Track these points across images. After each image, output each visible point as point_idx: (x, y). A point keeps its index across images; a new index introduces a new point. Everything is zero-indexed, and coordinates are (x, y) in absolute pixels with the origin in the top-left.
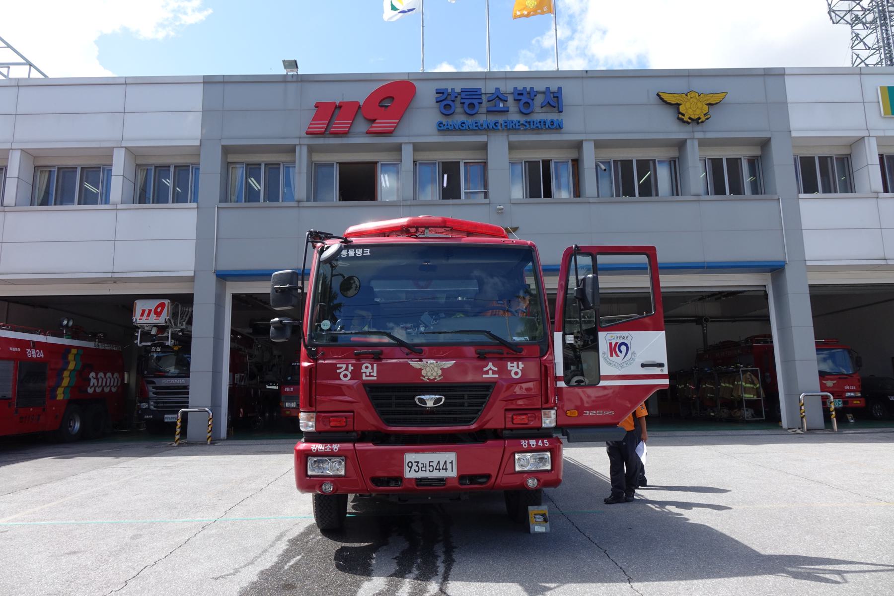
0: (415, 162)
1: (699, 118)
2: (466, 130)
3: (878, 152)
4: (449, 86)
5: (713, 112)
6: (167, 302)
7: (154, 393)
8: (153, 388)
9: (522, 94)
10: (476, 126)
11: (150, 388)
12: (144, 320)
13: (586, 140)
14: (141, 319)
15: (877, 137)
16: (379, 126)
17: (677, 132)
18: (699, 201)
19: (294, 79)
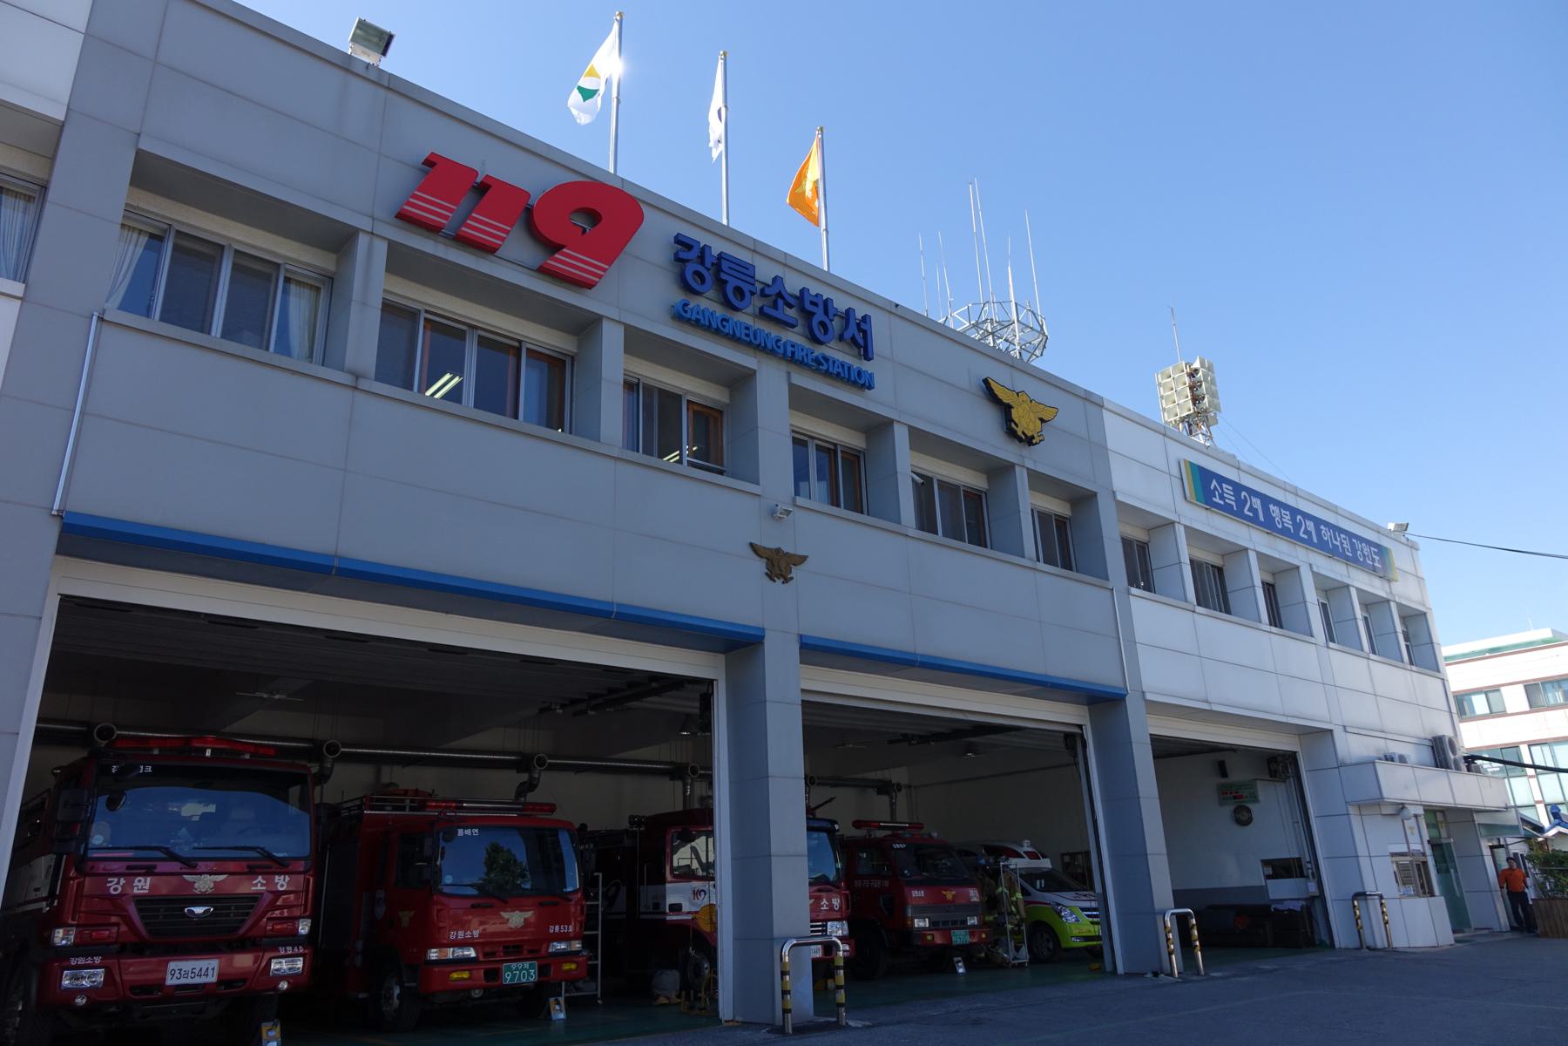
1: (1033, 437)
4: (703, 239)
9: (816, 304)
10: (747, 335)
13: (898, 422)
16: (561, 261)
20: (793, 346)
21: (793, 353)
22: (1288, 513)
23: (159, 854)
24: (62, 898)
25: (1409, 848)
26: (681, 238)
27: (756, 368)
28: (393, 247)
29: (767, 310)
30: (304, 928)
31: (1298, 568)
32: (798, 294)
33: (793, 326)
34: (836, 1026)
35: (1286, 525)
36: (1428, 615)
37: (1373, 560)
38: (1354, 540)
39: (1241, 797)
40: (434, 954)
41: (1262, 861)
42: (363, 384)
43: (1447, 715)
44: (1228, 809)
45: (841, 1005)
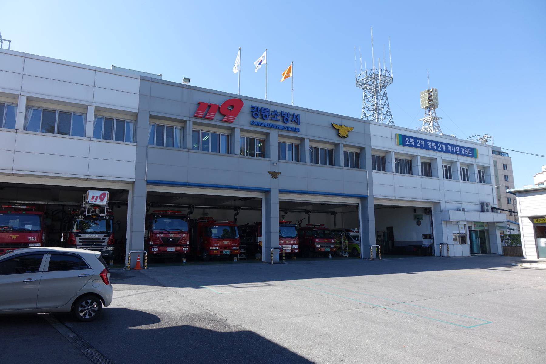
1: (345, 136)
2: (263, 126)
3: (395, 157)
5: (349, 134)
6: (107, 192)
7: (80, 242)
8: (80, 239)
9: (285, 115)
10: (268, 126)
11: (77, 239)
12: (93, 202)
14: (92, 201)
15: (395, 152)
17: (337, 140)
18: (343, 169)
19: (187, 87)
21: (279, 128)
23: (164, 230)
24: (150, 237)
25: (459, 232)
27: (270, 132)
29: (273, 119)
30: (188, 243)
34: (283, 263)
35: (433, 147)
37: (469, 153)
38: (461, 148)
39: (419, 218)
40: (211, 248)
43: (492, 196)
44: (416, 221)
45: (284, 260)
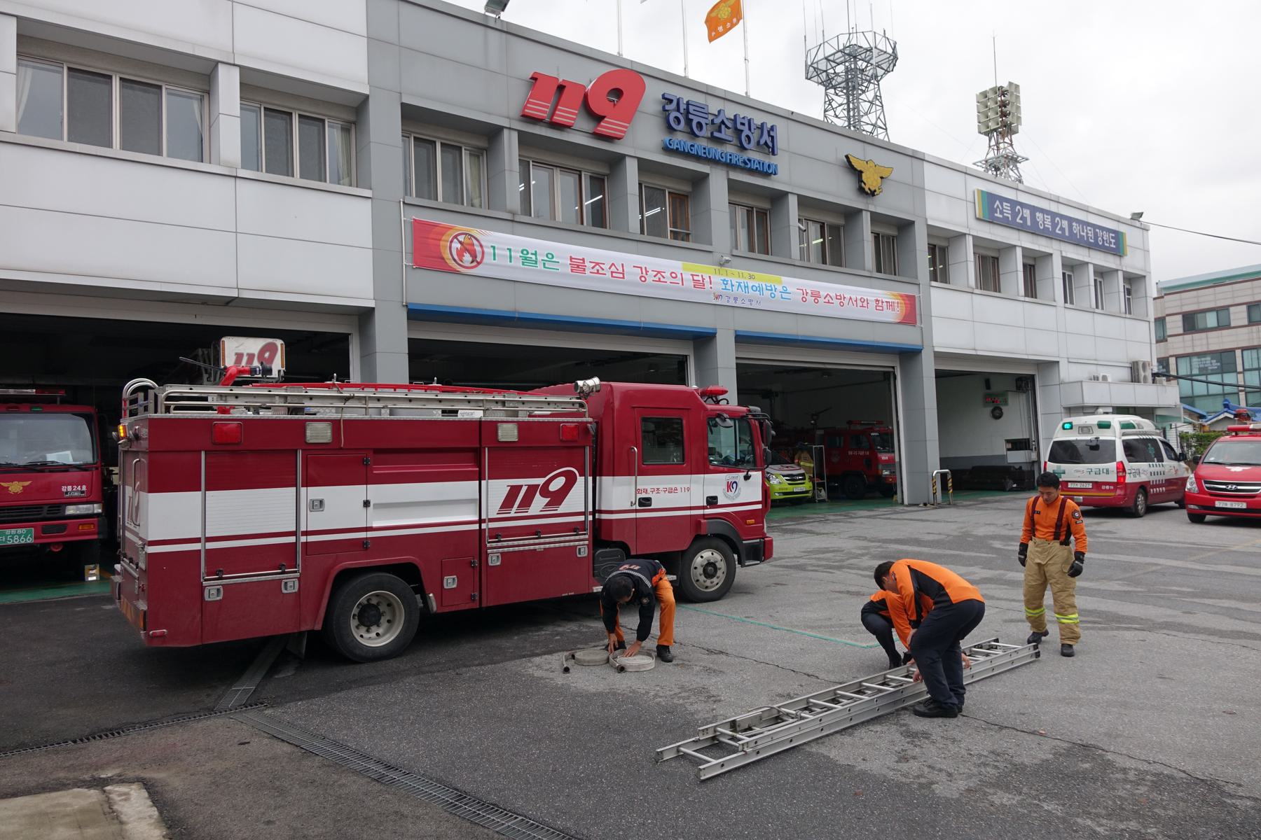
0: (640, 185)
1: (875, 191)
6: (279, 343)
9: (743, 124)
10: (705, 153)
16: (604, 128)
20: (730, 155)
21: (731, 160)
22: (1049, 217)
26: (666, 96)
28: (520, 132)
29: (716, 134)
31: (1051, 254)
32: (733, 118)
33: (730, 141)
35: (1046, 226)
36: (1147, 278)
37: (1110, 243)
38: (1097, 230)
41: (1006, 440)
42: (517, 219)
44: (989, 409)
